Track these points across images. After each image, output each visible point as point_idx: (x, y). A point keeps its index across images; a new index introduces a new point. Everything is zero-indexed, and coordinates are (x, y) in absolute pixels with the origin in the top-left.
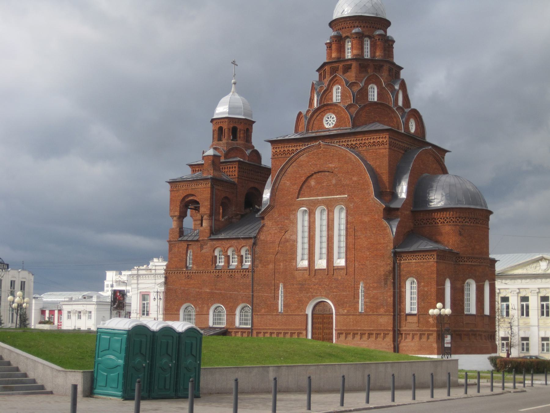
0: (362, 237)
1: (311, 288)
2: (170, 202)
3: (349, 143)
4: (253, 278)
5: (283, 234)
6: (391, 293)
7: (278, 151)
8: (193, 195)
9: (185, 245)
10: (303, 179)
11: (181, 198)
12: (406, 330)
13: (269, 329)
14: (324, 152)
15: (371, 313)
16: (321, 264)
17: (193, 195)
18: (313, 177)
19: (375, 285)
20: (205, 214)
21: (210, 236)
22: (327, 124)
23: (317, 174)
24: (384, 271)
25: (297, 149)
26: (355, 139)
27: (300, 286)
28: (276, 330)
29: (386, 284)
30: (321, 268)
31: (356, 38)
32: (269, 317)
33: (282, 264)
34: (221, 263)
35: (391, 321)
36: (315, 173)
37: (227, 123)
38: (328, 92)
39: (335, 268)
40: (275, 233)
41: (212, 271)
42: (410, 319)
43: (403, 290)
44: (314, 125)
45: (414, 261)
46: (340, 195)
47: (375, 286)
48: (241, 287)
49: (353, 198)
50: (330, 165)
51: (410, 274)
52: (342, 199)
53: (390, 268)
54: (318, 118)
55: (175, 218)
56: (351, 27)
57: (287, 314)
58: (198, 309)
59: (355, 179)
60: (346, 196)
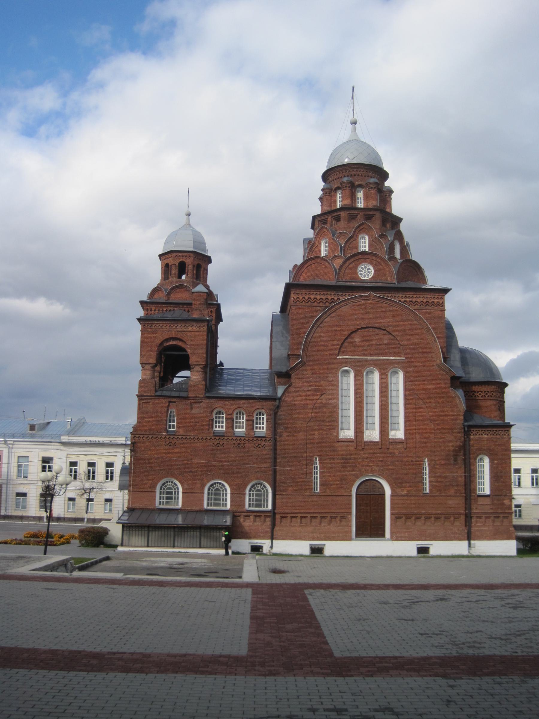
0: (424, 406)
1: (359, 464)
2: (141, 345)
3: (408, 300)
4: (275, 449)
5: (318, 397)
6: (461, 472)
7: (301, 298)
8: (180, 340)
9: (165, 402)
10: (346, 334)
11: (158, 341)
12: (478, 513)
13: (300, 513)
14: (374, 305)
15: (437, 494)
16: (373, 434)
17: (180, 340)
18: (358, 333)
19: (443, 462)
20: (198, 365)
21: (205, 394)
22: (369, 272)
23: (363, 331)
24: (453, 446)
25: (339, 299)
26: (404, 296)
27: (342, 461)
28: (319, 513)
29: (455, 461)
30: (372, 440)
31: (375, 188)
32: (300, 498)
33: (316, 433)
35: (462, 503)
36: (362, 328)
37: (192, 259)
38: (352, 239)
39: (390, 441)
41: (209, 438)
42: (481, 501)
43: (472, 468)
44: (346, 274)
45: (486, 436)
46: (395, 357)
47: (443, 463)
48: (254, 460)
50: (382, 321)
51: (482, 451)
52: (398, 362)
54: (351, 266)
55: (147, 367)
56: (365, 176)
57: (324, 494)
58: (186, 486)
59: (414, 340)
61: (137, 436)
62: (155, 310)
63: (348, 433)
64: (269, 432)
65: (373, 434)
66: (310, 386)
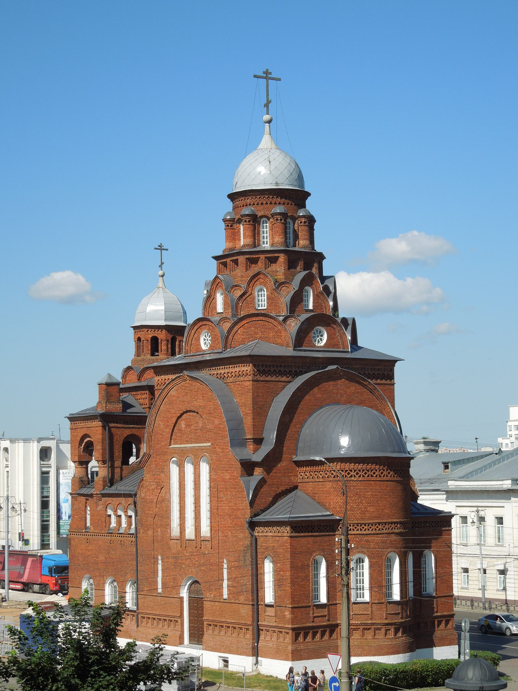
0: (224, 499)
10: (174, 420)
27: (174, 560)
34: (113, 525)
45: (271, 534)
54: (196, 335)
60: (209, 444)
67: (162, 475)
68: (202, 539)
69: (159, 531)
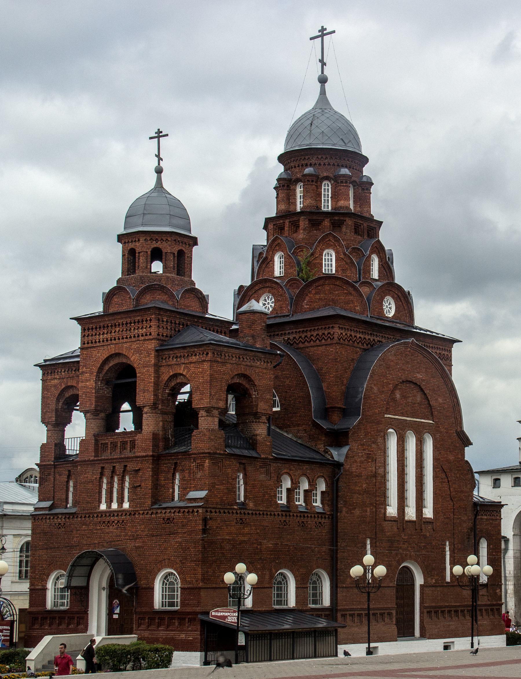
33: (368, 510)
40: (361, 462)
45: (485, 517)
49: (439, 427)
53: (470, 525)
61: (209, 510)
62: (167, 322)
63: (392, 510)
64: (327, 508)
65: (411, 513)
66: (364, 450)
67: (373, 446)
68: (424, 520)
69: (368, 510)
